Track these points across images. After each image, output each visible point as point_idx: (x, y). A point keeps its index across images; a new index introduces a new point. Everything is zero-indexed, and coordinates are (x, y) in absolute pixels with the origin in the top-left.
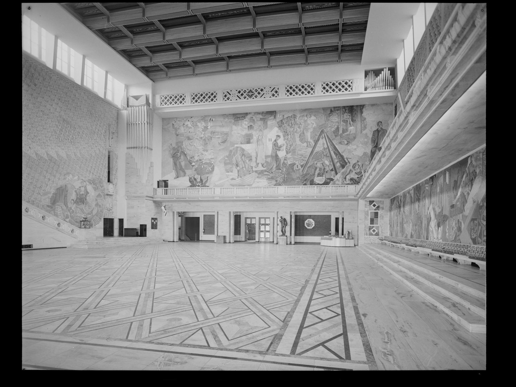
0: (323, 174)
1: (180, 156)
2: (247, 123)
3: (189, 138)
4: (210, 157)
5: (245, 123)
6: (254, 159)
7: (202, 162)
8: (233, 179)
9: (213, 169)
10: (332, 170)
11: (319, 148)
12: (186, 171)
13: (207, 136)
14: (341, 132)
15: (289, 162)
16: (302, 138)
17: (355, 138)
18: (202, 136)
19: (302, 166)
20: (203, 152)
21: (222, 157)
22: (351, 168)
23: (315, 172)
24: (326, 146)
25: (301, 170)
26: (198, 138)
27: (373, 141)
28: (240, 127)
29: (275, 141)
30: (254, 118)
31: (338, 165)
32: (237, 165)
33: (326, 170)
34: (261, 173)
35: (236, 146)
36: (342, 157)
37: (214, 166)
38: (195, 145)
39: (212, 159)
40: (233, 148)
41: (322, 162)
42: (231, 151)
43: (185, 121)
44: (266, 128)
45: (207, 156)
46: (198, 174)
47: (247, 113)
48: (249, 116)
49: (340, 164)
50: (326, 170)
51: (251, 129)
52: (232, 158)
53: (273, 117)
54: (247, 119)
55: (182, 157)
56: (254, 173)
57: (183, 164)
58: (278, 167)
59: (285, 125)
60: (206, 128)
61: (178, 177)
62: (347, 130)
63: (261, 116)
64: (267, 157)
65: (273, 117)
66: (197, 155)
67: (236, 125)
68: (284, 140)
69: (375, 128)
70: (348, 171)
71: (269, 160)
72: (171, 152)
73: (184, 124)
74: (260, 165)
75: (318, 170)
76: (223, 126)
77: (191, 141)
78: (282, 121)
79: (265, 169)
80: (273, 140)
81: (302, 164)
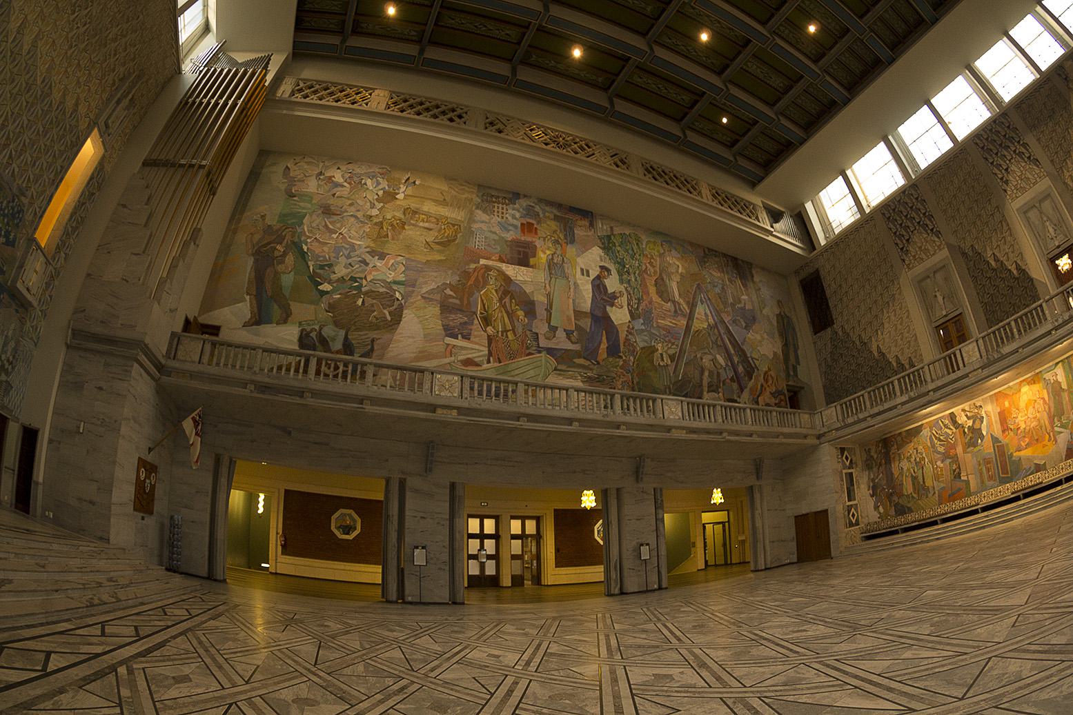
0: (718, 387)
1: (285, 254)
2: (518, 215)
3: (327, 211)
4: (391, 276)
5: (514, 214)
6: (541, 312)
7: (359, 288)
8: (469, 362)
9: (397, 317)
10: (732, 379)
11: (699, 324)
12: (295, 307)
13: (389, 216)
14: (731, 300)
15: (640, 342)
16: (663, 293)
17: (754, 319)
18: (375, 212)
19: (672, 357)
20: (368, 258)
21: (433, 286)
22: (762, 380)
23: (702, 380)
24: (711, 321)
25: (671, 369)
26: (359, 214)
27: (781, 335)
28: (496, 219)
29: (598, 277)
30: (537, 208)
31: (740, 369)
32: (487, 321)
33: (722, 379)
34: (563, 359)
35: (482, 262)
36: (743, 351)
37: (401, 309)
38: (344, 230)
39: (395, 282)
40: (473, 266)
41: (710, 357)
42: (466, 274)
43: (327, 168)
44: (572, 241)
45: (385, 271)
46: (337, 324)
47: (518, 194)
48: (524, 202)
49: (743, 367)
50: (722, 379)
51: (530, 231)
52: (471, 294)
53: (586, 223)
54: (517, 206)
55: (290, 259)
56: (543, 354)
57: (287, 280)
58: (613, 350)
59: (619, 248)
60: (390, 196)
61: (258, 323)
62: (740, 302)
63: (555, 212)
64: (578, 314)
65: (588, 224)
66: (343, 260)
67: (485, 211)
68: (621, 281)
69: (777, 312)
70: (759, 387)
71: (587, 323)
72: (257, 237)
73: (321, 173)
74: (561, 334)
75: (706, 373)
76: (444, 203)
77: (336, 218)
78: (609, 237)
79: (577, 347)
80: (594, 273)
81: (671, 352)
